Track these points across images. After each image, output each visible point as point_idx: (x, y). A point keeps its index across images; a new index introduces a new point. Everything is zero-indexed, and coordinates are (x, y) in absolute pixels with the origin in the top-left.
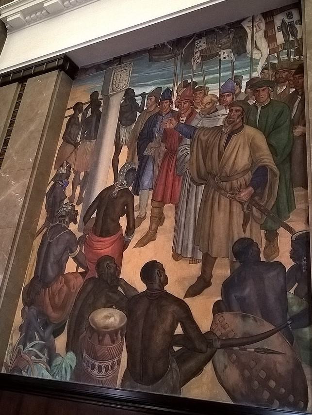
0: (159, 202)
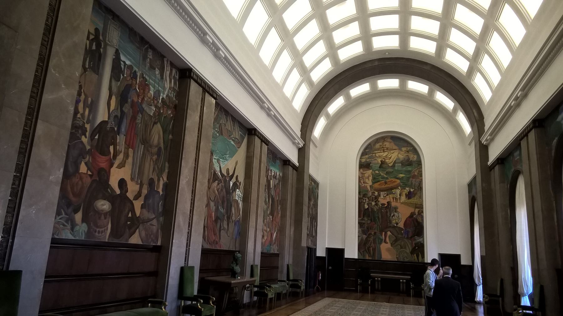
0: (129, 145)
